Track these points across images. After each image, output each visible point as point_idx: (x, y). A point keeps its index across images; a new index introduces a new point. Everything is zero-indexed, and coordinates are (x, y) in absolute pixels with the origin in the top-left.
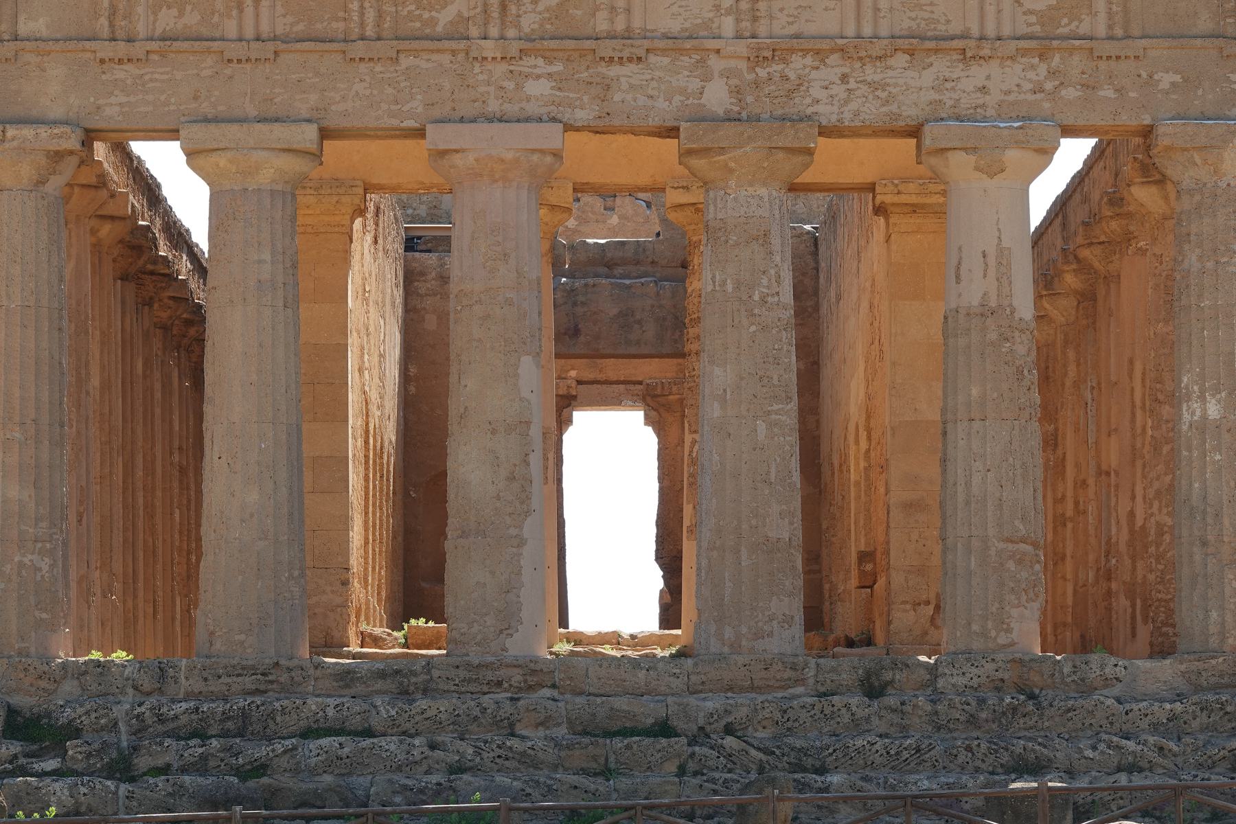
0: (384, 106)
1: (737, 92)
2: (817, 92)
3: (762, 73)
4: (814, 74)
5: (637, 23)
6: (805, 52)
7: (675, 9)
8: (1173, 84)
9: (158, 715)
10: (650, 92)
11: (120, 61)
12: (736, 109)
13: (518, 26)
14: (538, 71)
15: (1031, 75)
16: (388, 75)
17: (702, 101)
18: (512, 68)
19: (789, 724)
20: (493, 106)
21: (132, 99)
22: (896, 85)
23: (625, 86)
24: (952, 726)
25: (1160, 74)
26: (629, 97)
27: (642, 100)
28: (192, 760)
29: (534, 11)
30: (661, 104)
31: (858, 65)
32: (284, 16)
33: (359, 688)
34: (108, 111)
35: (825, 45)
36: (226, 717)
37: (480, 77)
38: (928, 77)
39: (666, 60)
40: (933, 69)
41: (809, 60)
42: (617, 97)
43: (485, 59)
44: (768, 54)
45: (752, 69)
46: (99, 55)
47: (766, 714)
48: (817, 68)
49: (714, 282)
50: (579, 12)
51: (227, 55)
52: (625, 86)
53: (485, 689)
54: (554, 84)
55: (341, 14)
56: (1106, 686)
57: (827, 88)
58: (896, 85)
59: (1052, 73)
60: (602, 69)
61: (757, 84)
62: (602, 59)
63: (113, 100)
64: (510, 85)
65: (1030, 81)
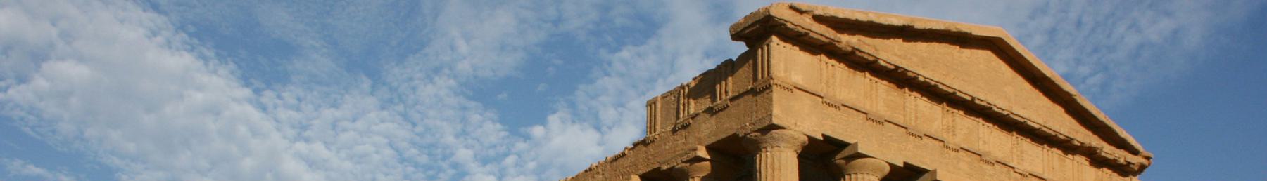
46: (825, 100)
51: (869, 116)
55: (902, 112)
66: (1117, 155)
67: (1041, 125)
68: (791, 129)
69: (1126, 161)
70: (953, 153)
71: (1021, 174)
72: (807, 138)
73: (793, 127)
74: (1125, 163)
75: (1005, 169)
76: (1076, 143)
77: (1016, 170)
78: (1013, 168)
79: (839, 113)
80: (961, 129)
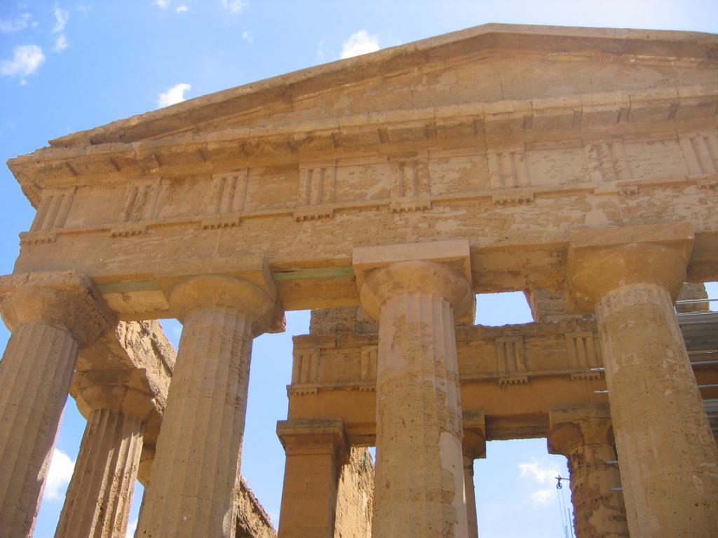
3: (632, 203)
4: (676, 201)
5: (523, 180)
6: (664, 185)
10: (540, 222)
11: (127, 235)
13: (429, 191)
16: (326, 227)
17: (586, 224)
18: (425, 215)
26: (523, 226)
27: (534, 227)
30: (551, 228)
31: (711, 192)
32: (251, 202)
37: (400, 223)
39: (550, 201)
41: (669, 192)
42: (514, 227)
43: (402, 210)
45: (622, 202)
46: (112, 232)
49: (620, 364)
50: (476, 181)
51: (204, 223)
54: (459, 222)
57: (689, 208)
60: (498, 210)
64: (424, 226)
70: (415, 217)
75: (566, 200)
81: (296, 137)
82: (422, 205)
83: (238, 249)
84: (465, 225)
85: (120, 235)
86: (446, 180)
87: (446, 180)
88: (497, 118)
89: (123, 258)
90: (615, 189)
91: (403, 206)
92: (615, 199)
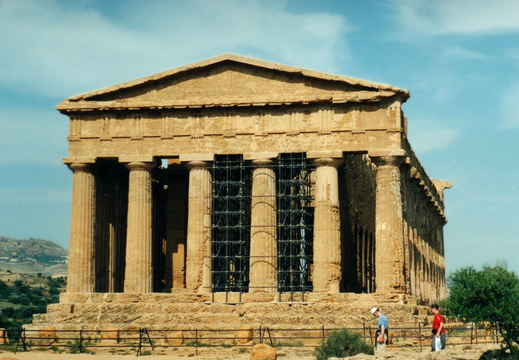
0: (170, 150)
1: (259, 144)
2: (279, 144)
3: (265, 139)
4: (279, 140)
7: (244, 123)
8: (373, 139)
9: (109, 308)
10: (237, 145)
11: (106, 140)
12: (259, 149)
14: (209, 140)
15: (335, 138)
19: (267, 311)
20: (198, 149)
21: (108, 150)
22: (300, 142)
23: (230, 144)
24: (310, 312)
25: (370, 137)
27: (235, 148)
28: (114, 320)
29: (208, 125)
33: (160, 301)
34: (103, 153)
35: (282, 132)
36: (125, 308)
38: (309, 139)
40: (310, 138)
41: (278, 135)
43: (195, 137)
44: (267, 134)
46: (100, 139)
47: (261, 308)
48: (279, 138)
52: (230, 144)
53: (192, 301)
56: (353, 302)
58: (300, 142)
59: (341, 137)
60: (225, 139)
61: (264, 142)
62: (225, 137)
63: (104, 150)
64: (201, 144)
65: (335, 140)
66: (349, 99)
67: (265, 103)
68: (74, 163)
69: (360, 100)
70: (199, 140)
71: (261, 136)
72: (85, 165)
73: (74, 162)
74: (360, 101)
75: (246, 137)
76: (304, 103)
77: (255, 135)
78: (253, 134)
79: (112, 142)
80: (208, 122)
81: (159, 108)
82: (201, 136)
83: (144, 149)
84: (214, 145)
85: (103, 140)
86: (210, 124)
87: (210, 124)
88: (226, 106)
89: (106, 150)
90: (260, 134)
91: (195, 136)
92: (261, 137)
